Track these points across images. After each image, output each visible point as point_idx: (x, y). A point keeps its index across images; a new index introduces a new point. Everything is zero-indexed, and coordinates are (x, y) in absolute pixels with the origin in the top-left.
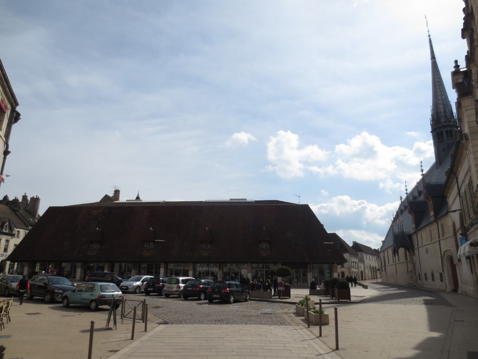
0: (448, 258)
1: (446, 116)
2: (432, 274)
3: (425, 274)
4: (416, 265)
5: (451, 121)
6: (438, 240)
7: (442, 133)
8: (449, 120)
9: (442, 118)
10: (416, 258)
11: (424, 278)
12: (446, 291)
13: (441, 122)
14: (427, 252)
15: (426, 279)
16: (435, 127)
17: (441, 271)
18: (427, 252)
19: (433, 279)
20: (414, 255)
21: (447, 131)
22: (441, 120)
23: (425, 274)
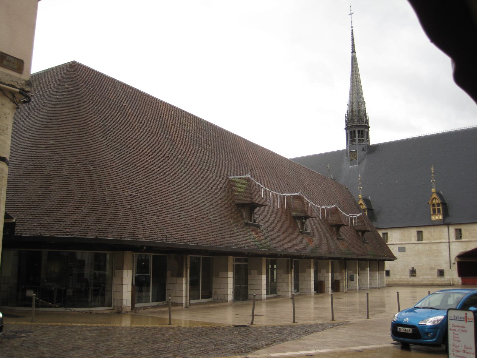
13: (363, 121)
16: (357, 123)
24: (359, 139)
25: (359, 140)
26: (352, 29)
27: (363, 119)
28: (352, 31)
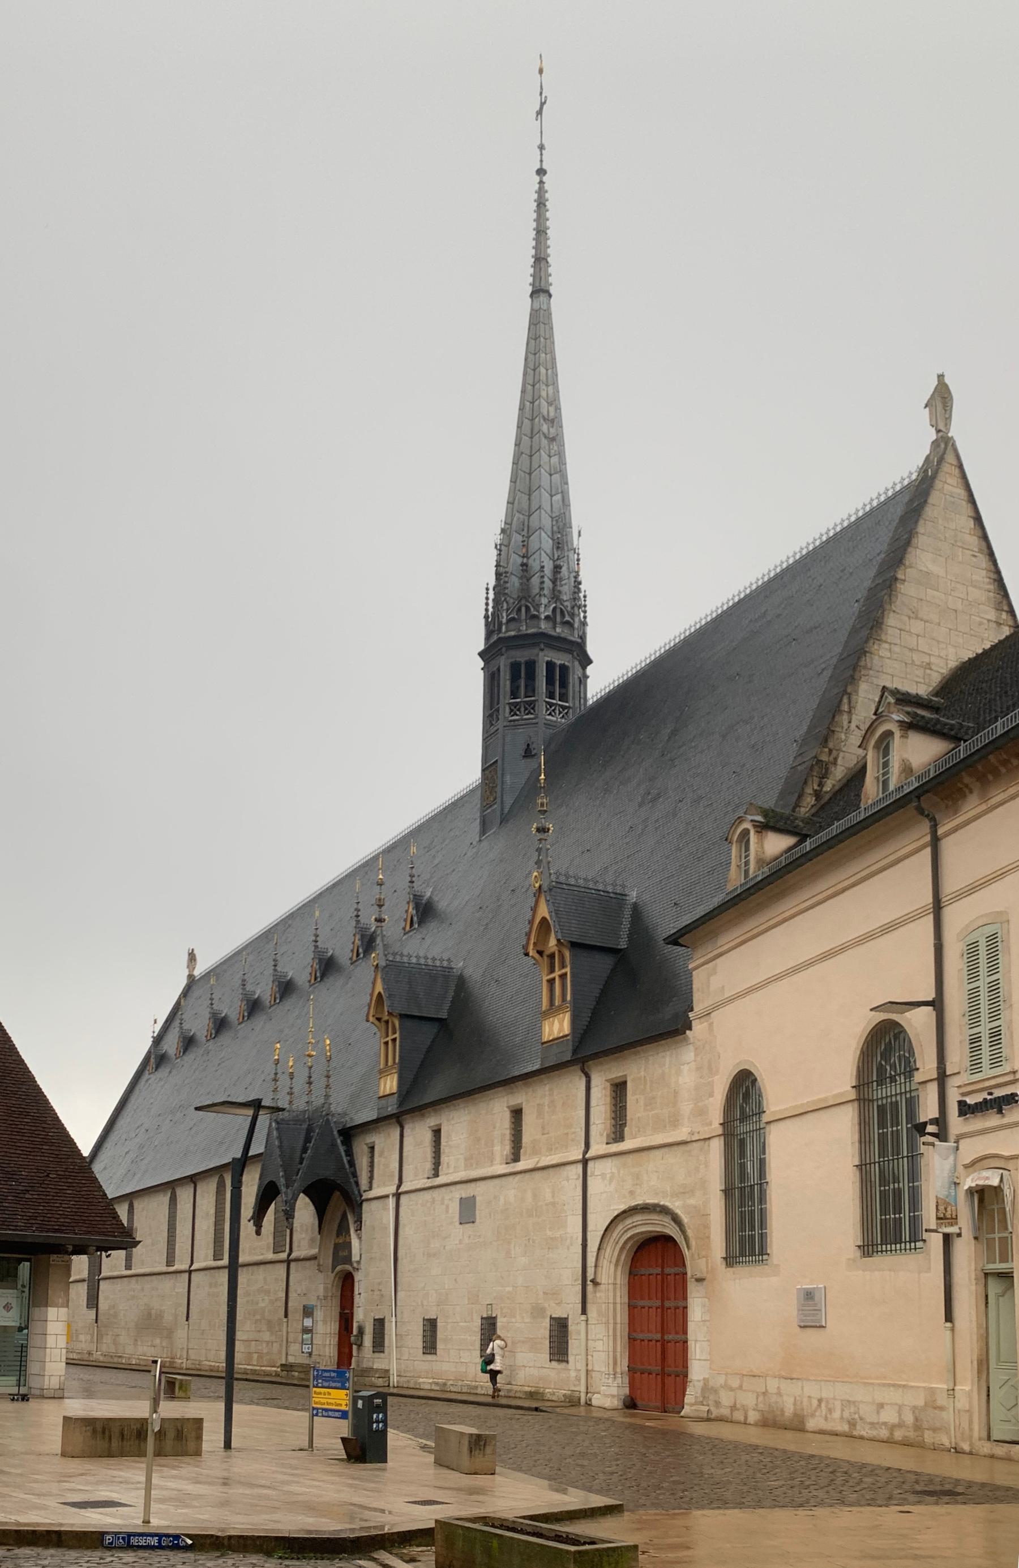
1: (556, 596)
4: (358, 1277)
5: (570, 624)
6: (581, 1157)
7: (531, 665)
8: (567, 618)
9: (544, 601)
11: (417, 1341)
12: (589, 1404)
13: (536, 617)
16: (506, 631)
17: (569, 1306)
20: (359, 1229)
21: (550, 665)
22: (539, 605)
24: (516, 704)
25: (514, 709)
26: (541, 182)
27: (537, 607)
28: (541, 191)
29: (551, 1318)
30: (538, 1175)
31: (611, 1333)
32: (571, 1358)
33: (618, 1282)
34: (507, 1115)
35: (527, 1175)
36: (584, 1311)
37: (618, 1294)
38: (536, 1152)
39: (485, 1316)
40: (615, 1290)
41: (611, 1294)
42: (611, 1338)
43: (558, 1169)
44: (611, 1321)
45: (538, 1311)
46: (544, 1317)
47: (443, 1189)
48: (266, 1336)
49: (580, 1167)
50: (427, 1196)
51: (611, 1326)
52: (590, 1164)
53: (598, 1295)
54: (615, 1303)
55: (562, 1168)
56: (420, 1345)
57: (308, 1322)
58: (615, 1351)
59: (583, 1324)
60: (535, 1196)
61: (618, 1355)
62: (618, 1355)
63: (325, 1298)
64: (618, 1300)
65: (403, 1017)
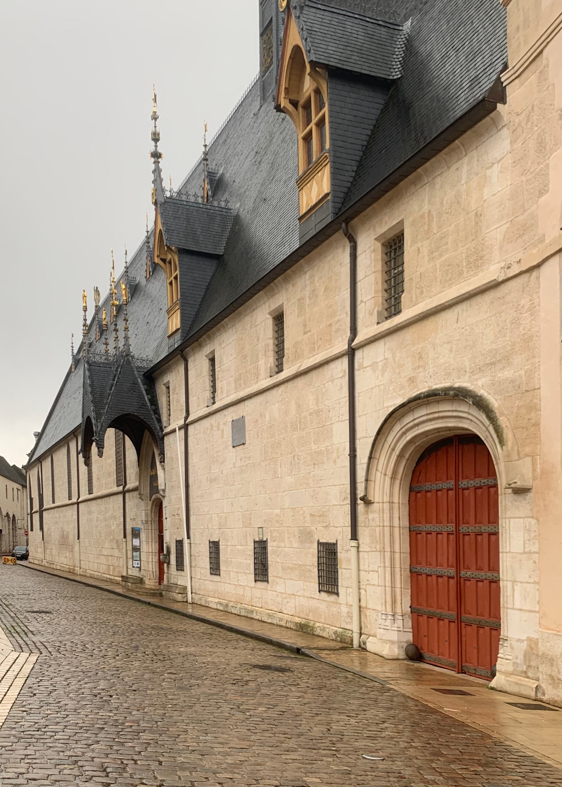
0: (407, 456)
2: (261, 549)
3: (215, 547)
6: (346, 347)
10: (169, 476)
11: (205, 562)
12: (362, 648)
14: (239, 441)
15: (215, 569)
17: (337, 531)
18: (239, 441)
19: (261, 571)
23: (215, 547)
29: (319, 543)
30: (300, 382)
31: (388, 564)
32: (341, 590)
33: (396, 500)
34: (270, 322)
35: (290, 385)
36: (354, 536)
37: (396, 516)
38: (298, 356)
39: (257, 539)
40: (391, 509)
41: (387, 516)
42: (388, 570)
43: (321, 370)
44: (388, 549)
45: (305, 535)
46: (312, 542)
47: (218, 415)
48: (116, 553)
49: (345, 361)
50: (206, 423)
51: (388, 555)
52: (358, 355)
53: (371, 516)
54: (392, 527)
55: (326, 367)
56: (208, 566)
57: (136, 542)
58: (393, 587)
59: (354, 550)
60: (299, 406)
61: (398, 591)
62: (398, 591)
63: (147, 522)
64: (396, 523)
65: (182, 252)
